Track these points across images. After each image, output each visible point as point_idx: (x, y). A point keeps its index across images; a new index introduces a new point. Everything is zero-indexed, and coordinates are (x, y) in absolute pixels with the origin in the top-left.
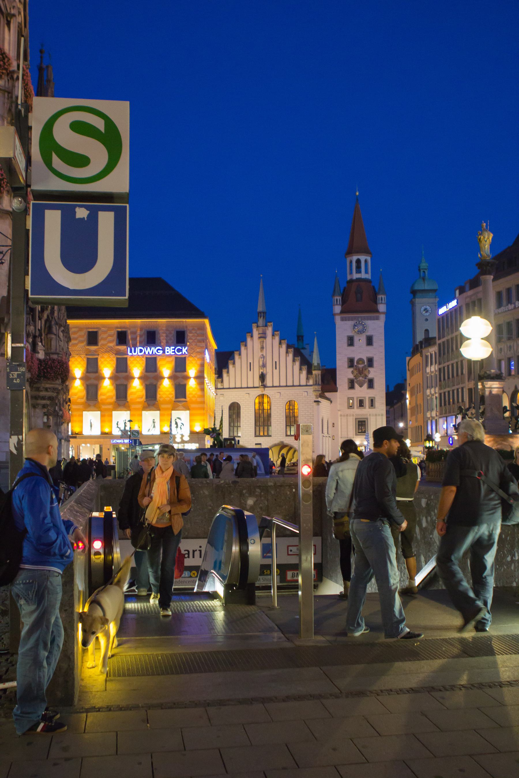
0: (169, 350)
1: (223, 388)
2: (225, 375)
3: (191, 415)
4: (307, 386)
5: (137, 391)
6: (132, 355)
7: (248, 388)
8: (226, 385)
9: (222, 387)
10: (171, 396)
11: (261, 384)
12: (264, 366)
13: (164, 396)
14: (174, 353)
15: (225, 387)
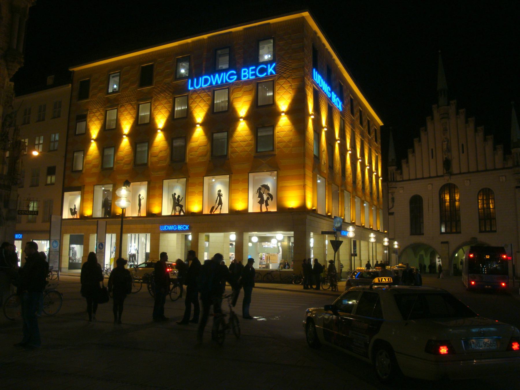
0: (246, 73)
1: (403, 181)
2: (404, 166)
3: (279, 179)
4: (504, 168)
5: (199, 146)
6: (195, 91)
7: (430, 177)
8: (406, 177)
9: (401, 179)
10: (248, 149)
11: (445, 172)
12: (449, 150)
13: (238, 150)
14: (254, 77)
15: (405, 178)
